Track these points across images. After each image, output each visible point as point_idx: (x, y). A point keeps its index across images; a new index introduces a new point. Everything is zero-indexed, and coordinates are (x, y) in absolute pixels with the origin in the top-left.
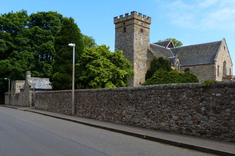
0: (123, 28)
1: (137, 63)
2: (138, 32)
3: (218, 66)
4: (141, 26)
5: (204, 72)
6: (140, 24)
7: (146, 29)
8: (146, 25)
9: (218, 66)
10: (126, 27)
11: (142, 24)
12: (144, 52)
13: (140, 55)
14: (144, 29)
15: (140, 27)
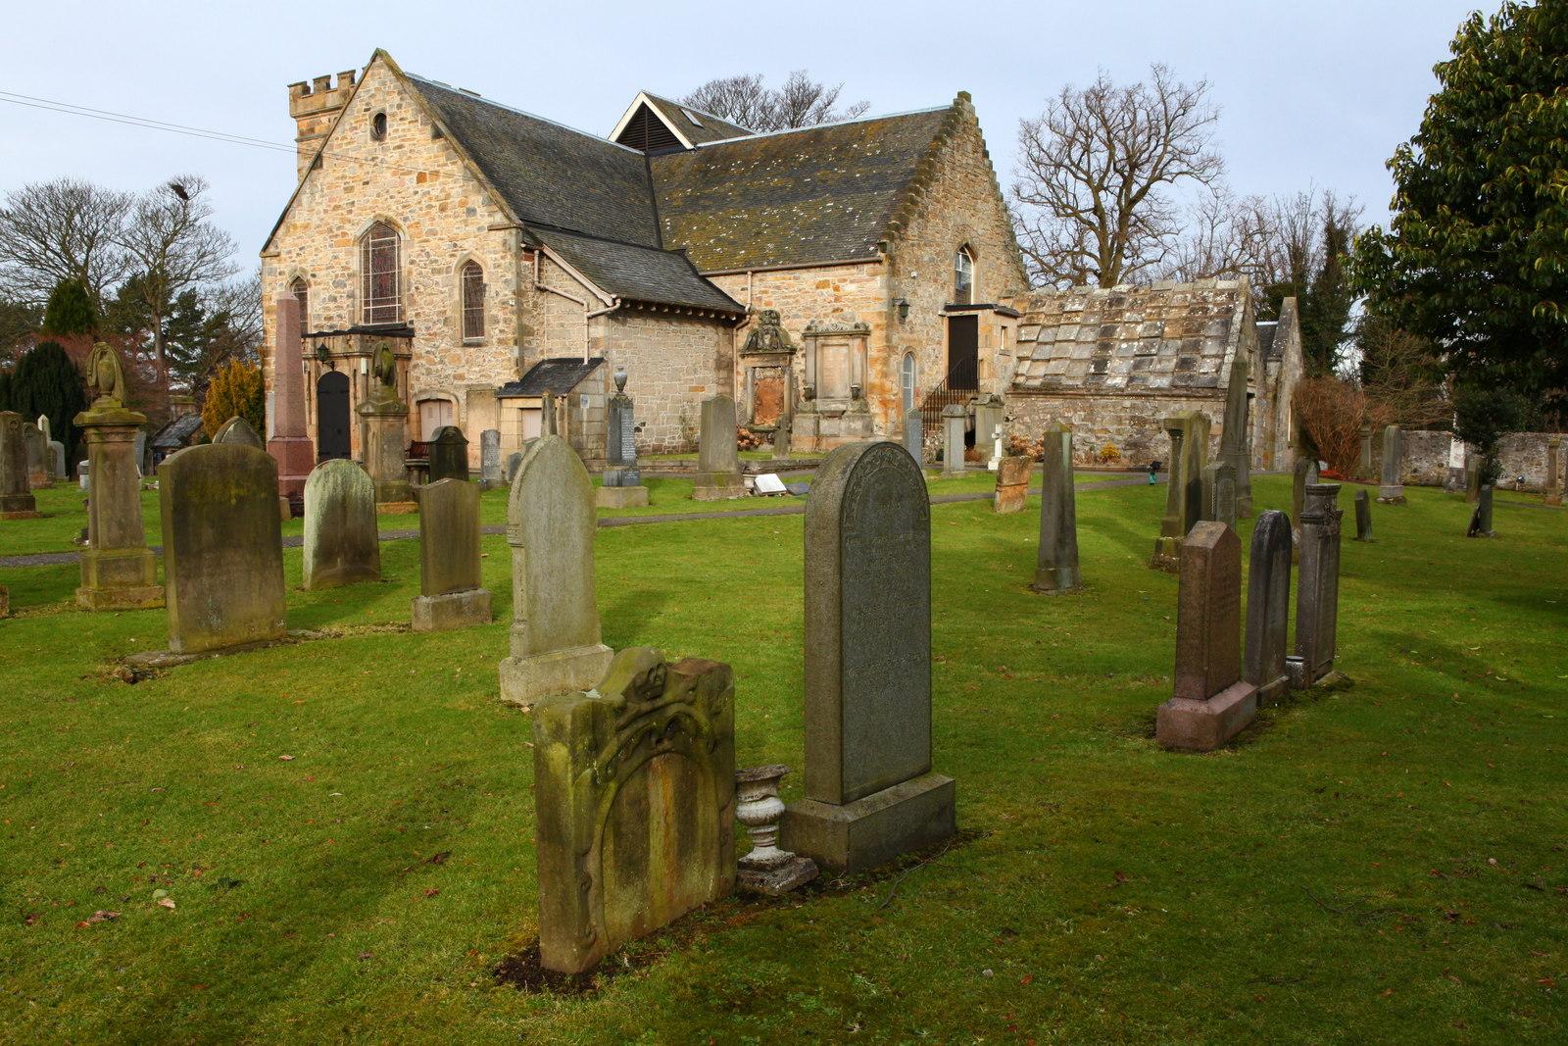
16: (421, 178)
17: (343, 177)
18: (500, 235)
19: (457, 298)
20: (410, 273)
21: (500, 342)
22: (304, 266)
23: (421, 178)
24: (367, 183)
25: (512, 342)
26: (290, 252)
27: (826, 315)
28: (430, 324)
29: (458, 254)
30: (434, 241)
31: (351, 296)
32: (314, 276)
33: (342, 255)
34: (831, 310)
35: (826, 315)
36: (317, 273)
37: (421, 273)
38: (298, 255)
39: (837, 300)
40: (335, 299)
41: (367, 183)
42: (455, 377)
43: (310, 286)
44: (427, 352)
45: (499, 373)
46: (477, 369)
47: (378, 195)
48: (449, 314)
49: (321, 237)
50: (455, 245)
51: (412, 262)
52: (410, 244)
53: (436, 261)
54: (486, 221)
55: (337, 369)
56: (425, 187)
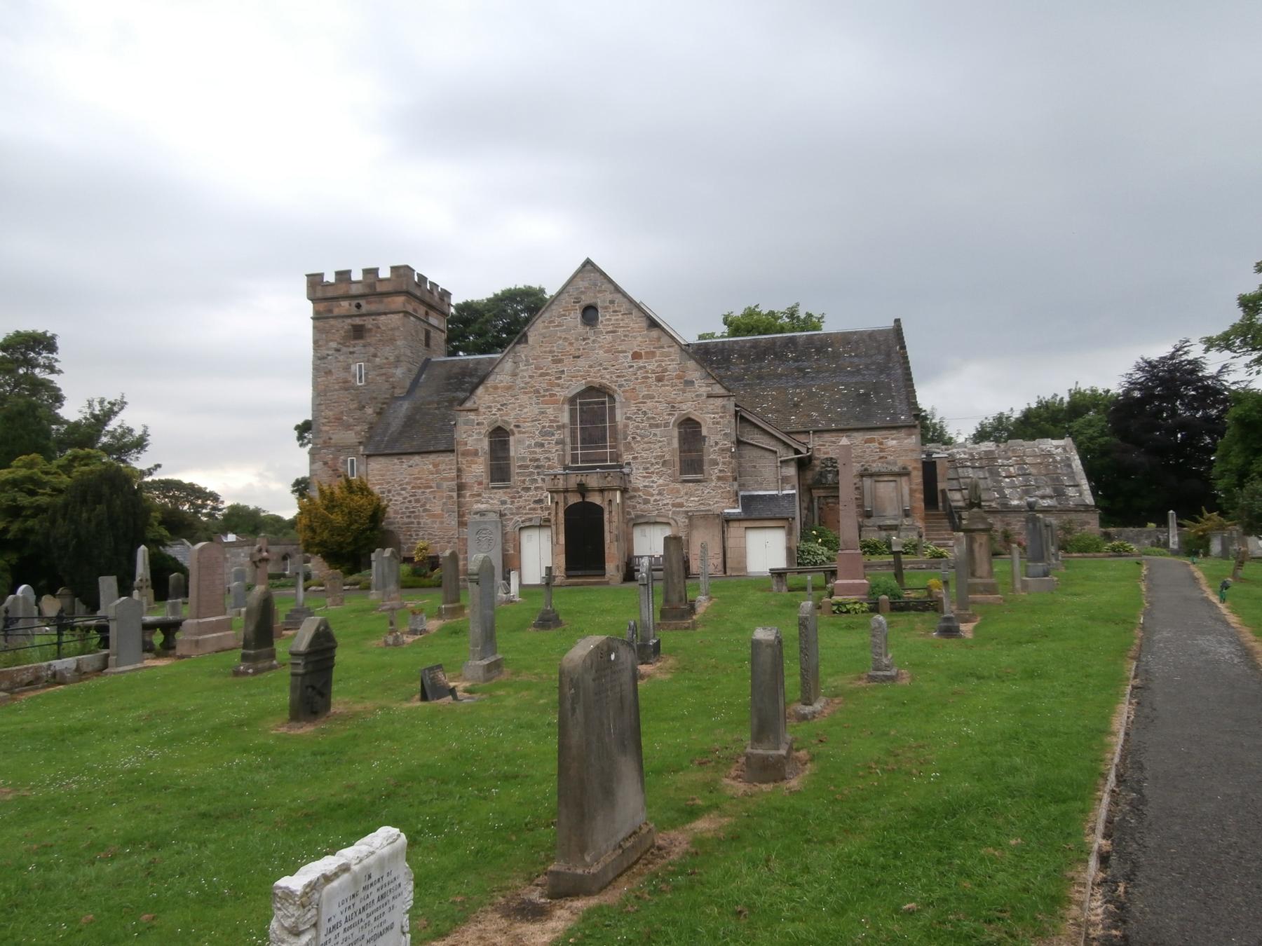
1: (325, 463)
3: (499, 436)
7: (383, 318)
8: (381, 302)
9: (499, 436)
11: (358, 306)
13: (348, 427)
14: (369, 322)
15: (349, 321)
16: (636, 356)
17: (551, 352)
18: (719, 402)
20: (626, 426)
21: (719, 478)
22: (505, 418)
24: (578, 357)
25: (731, 479)
26: (490, 407)
27: (874, 461)
28: (649, 465)
31: (561, 442)
32: (517, 426)
33: (550, 411)
34: (878, 457)
35: (874, 461)
37: (637, 428)
38: (499, 409)
39: (882, 450)
40: (542, 445)
41: (578, 357)
42: (674, 505)
43: (513, 434)
44: (645, 486)
46: (696, 499)
47: (591, 367)
48: (667, 457)
49: (526, 397)
50: (673, 407)
51: (628, 418)
52: (626, 405)
53: (653, 418)
54: (704, 390)
55: (588, 500)
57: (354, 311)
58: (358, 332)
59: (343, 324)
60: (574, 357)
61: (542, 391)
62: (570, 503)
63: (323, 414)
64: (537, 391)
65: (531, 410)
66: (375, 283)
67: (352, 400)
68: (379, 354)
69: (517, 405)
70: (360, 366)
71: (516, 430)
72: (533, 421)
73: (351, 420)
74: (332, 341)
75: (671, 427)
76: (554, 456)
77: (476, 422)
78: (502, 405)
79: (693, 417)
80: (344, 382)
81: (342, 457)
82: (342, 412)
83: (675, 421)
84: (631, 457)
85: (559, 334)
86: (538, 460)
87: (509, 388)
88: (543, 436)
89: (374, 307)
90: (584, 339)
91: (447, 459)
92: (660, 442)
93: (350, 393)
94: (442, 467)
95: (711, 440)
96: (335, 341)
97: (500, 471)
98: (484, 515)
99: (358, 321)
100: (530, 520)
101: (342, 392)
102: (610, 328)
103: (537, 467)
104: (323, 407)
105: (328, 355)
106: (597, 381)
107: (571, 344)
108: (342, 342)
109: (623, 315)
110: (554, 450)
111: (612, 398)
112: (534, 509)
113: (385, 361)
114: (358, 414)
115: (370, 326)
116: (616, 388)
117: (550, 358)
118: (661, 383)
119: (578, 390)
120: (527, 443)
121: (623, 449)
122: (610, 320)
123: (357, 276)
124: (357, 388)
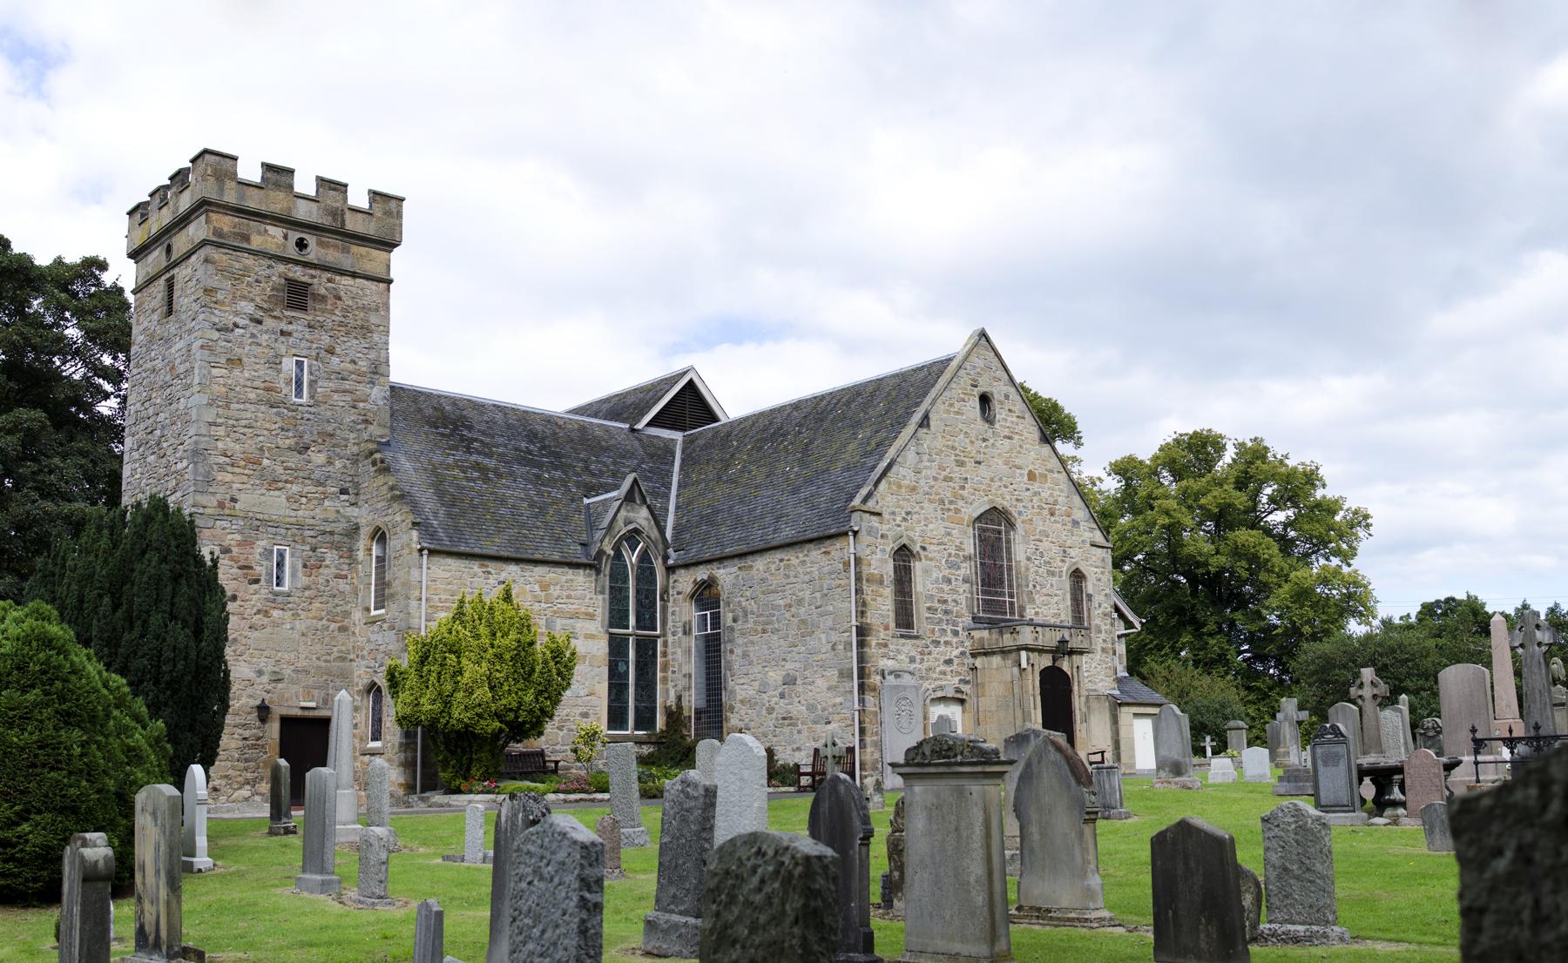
0: (164, 278)
2: (249, 308)
3: (904, 555)
4: (297, 262)
5: (800, 602)
6: (272, 248)
7: (347, 281)
8: (346, 251)
9: (904, 555)
10: (176, 271)
11: (301, 244)
12: (320, 459)
13: (274, 483)
14: (320, 283)
15: (281, 268)
19: (1069, 603)
20: (1027, 569)
22: (911, 533)
23: (1031, 476)
24: (979, 463)
26: (893, 513)
29: (1067, 560)
30: (1045, 545)
36: (927, 546)
37: (1037, 572)
38: (905, 519)
41: (979, 463)
45: (1102, 680)
54: (1087, 535)
56: (1036, 486)
57: (292, 252)
58: (297, 296)
59: (268, 271)
60: (976, 462)
61: (946, 502)
62: (1042, 667)
63: (220, 445)
64: (942, 502)
65: (936, 529)
66: (343, 214)
67: (283, 429)
68: (338, 350)
69: (922, 516)
70: (299, 364)
71: (922, 553)
72: (939, 544)
73: (280, 470)
74: (244, 297)
75: (1064, 578)
76: (962, 599)
77: (880, 532)
78: (908, 513)
79: (1081, 568)
80: (267, 389)
81: (263, 543)
82: (261, 449)
83: (1068, 570)
84: (1033, 611)
85: (960, 426)
86: (945, 602)
87: (913, 489)
88: (950, 568)
89: (332, 256)
90: (984, 440)
91: (564, 579)
92: (1056, 595)
93: (278, 414)
94: (555, 591)
95: (1097, 599)
96: (252, 300)
97: (904, 617)
98: (899, 676)
99: (298, 273)
100: (941, 688)
101: (263, 408)
102: (1006, 432)
103: (946, 612)
104: (221, 431)
105: (236, 325)
106: (1000, 503)
107: (972, 442)
108: (265, 306)
109: (1018, 417)
110: (961, 590)
111: (1011, 525)
112: (944, 673)
113: (351, 367)
114: (294, 460)
115: (322, 291)
116: (1016, 515)
117: (953, 457)
118: (1053, 519)
119: (982, 510)
120: (935, 575)
121: (1026, 599)
122: (1005, 420)
123: (304, 184)
124: (294, 408)
